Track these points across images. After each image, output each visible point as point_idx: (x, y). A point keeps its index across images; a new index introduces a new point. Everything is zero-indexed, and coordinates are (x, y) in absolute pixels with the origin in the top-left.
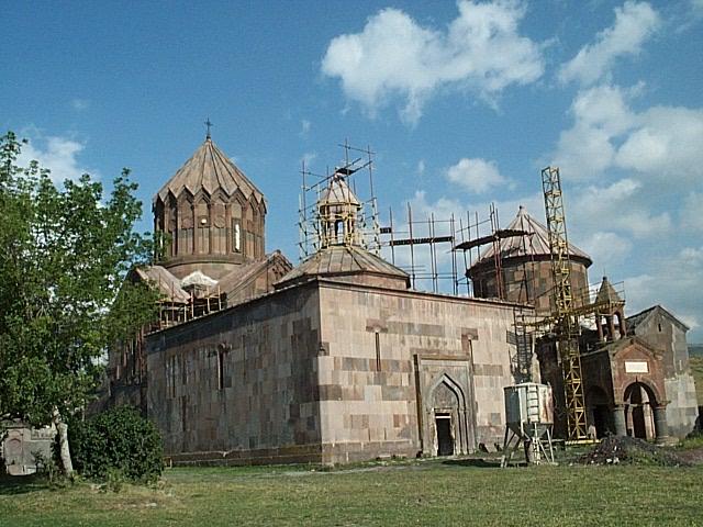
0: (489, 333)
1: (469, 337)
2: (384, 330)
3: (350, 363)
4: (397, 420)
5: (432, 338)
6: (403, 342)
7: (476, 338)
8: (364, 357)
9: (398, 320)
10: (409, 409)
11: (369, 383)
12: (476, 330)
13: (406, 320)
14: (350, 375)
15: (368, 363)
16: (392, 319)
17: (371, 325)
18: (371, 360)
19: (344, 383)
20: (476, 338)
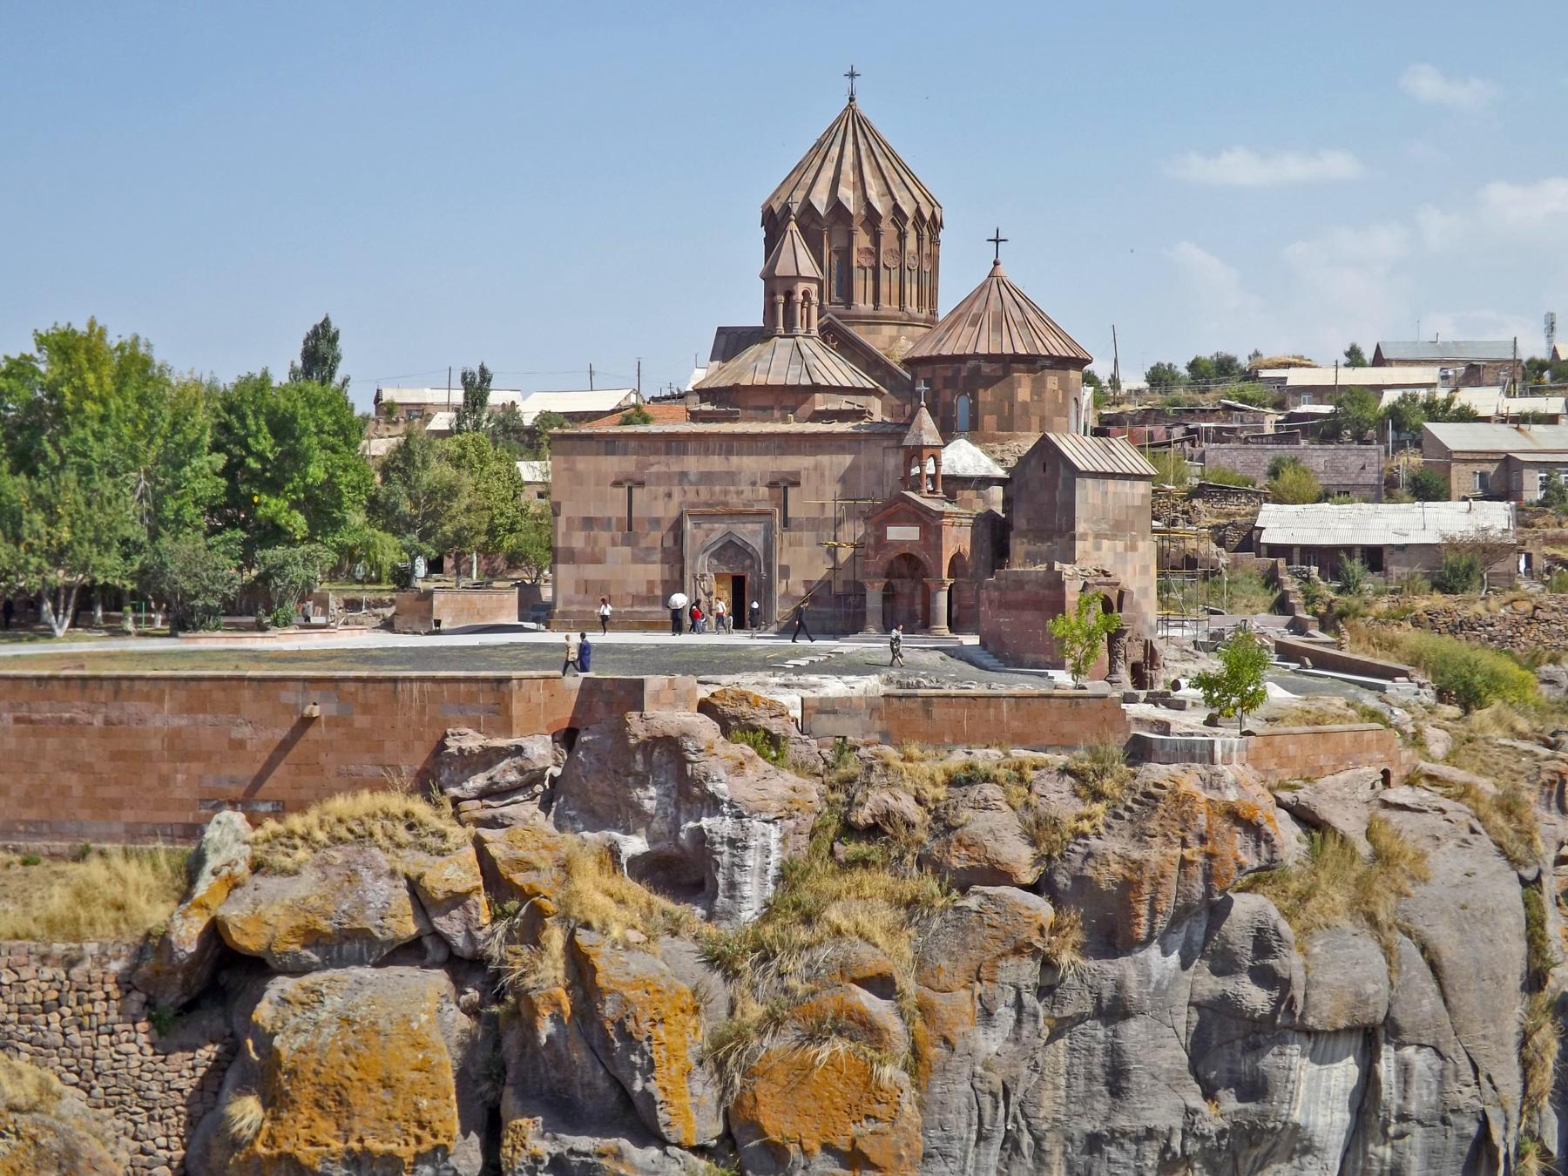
0: (822, 475)
1: (783, 485)
2: (641, 484)
3: (588, 523)
4: (651, 584)
5: (717, 488)
6: (669, 495)
7: (797, 484)
8: (608, 514)
9: (663, 469)
10: (672, 574)
11: (614, 544)
12: (798, 473)
13: (676, 468)
14: (588, 538)
15: (614, 521)
16: (654, 469)
17: (621, 478)
18: (619, 520)
19: (578, 541)
20: (797, 484)
